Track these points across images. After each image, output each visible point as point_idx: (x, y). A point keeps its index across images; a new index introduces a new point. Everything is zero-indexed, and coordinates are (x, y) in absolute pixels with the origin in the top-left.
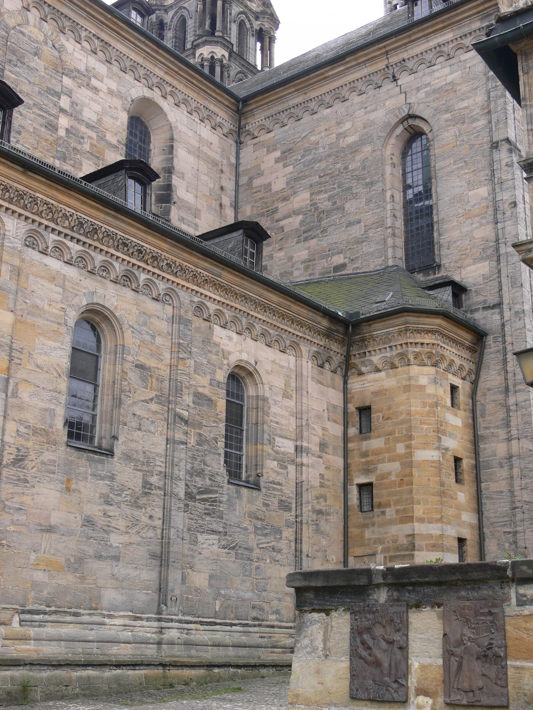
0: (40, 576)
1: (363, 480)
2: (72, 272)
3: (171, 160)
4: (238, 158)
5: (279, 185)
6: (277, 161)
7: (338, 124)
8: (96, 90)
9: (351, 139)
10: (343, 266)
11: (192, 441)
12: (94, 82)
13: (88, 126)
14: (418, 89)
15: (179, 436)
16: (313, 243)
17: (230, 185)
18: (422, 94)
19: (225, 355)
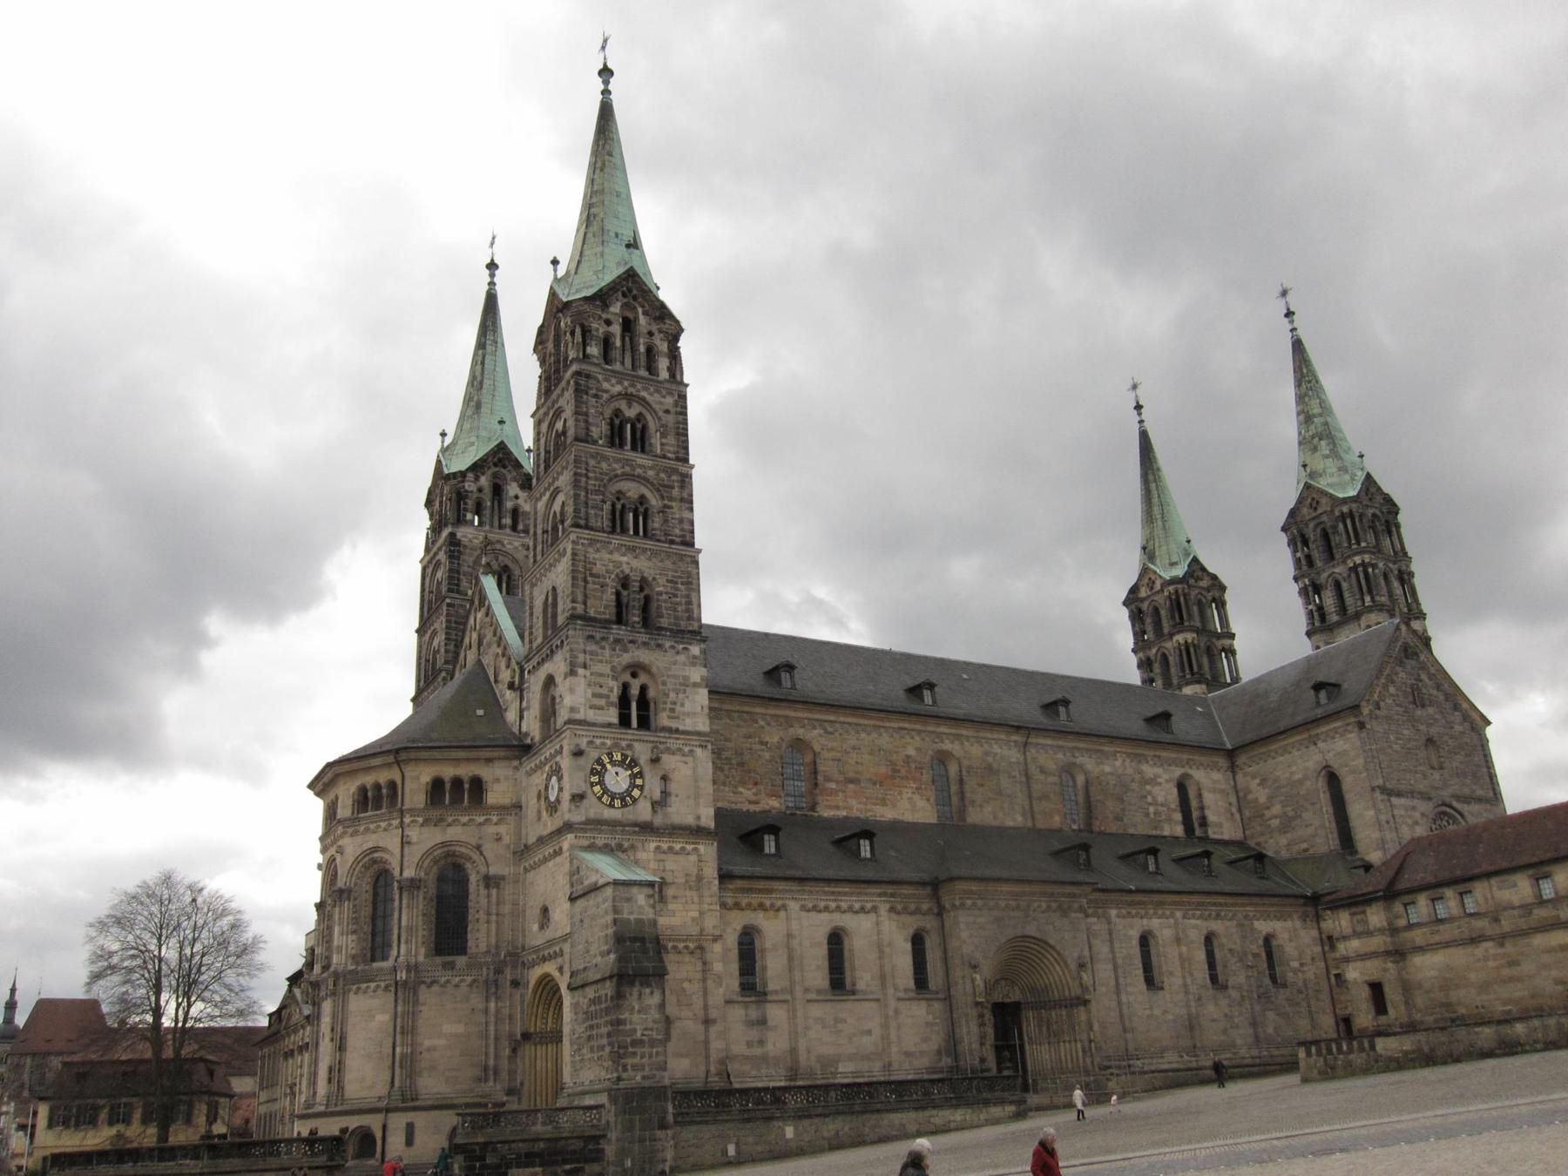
0: (1215, 1038)
1: (1336, 972)
2: (1199, 922)
3: (1202, 802)
4: (1235, 782)
5: (1262, 799)
6: (1259, 785)
7: (1289, 766)
8: (1160, 784)
9: (1298, 776)
10: (1306, 850)
11: (1255, 974)
12: (1159, 780)
13: (1162, 805)
14: (1329, 751)
15: (1250, 974)
16: (1289, 835)
17: (1233, 800)
18: (1331, 754)
19: (1260, 932)
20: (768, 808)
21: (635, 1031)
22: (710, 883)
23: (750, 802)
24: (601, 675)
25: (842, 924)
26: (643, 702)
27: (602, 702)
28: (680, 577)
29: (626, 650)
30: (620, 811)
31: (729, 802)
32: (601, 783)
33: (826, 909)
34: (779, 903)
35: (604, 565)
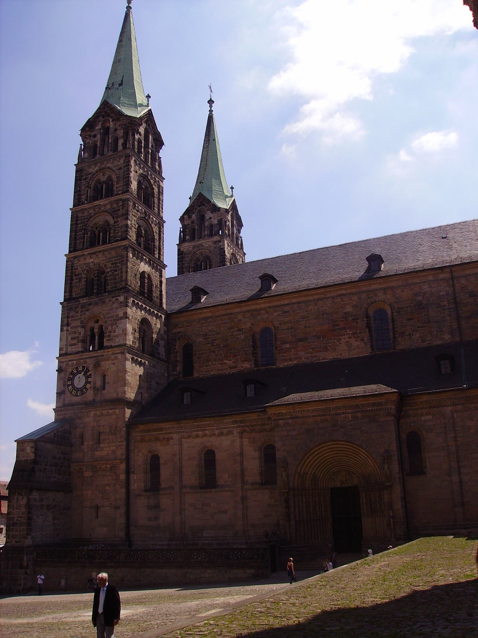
20: (242, 369)
21: (14, 518)
22: (121, 430)
23: (231, 368)
24: (76, 327)
25: (209, 444)
26: (102, 335)
27: (75, 341)
28: (118, 260)
29: (88, 310)
30: (80, 397)
31: (218, 370)
32: (72, 384)
33: (197, 436)
34: (168, 436)
35: (81, 268)
